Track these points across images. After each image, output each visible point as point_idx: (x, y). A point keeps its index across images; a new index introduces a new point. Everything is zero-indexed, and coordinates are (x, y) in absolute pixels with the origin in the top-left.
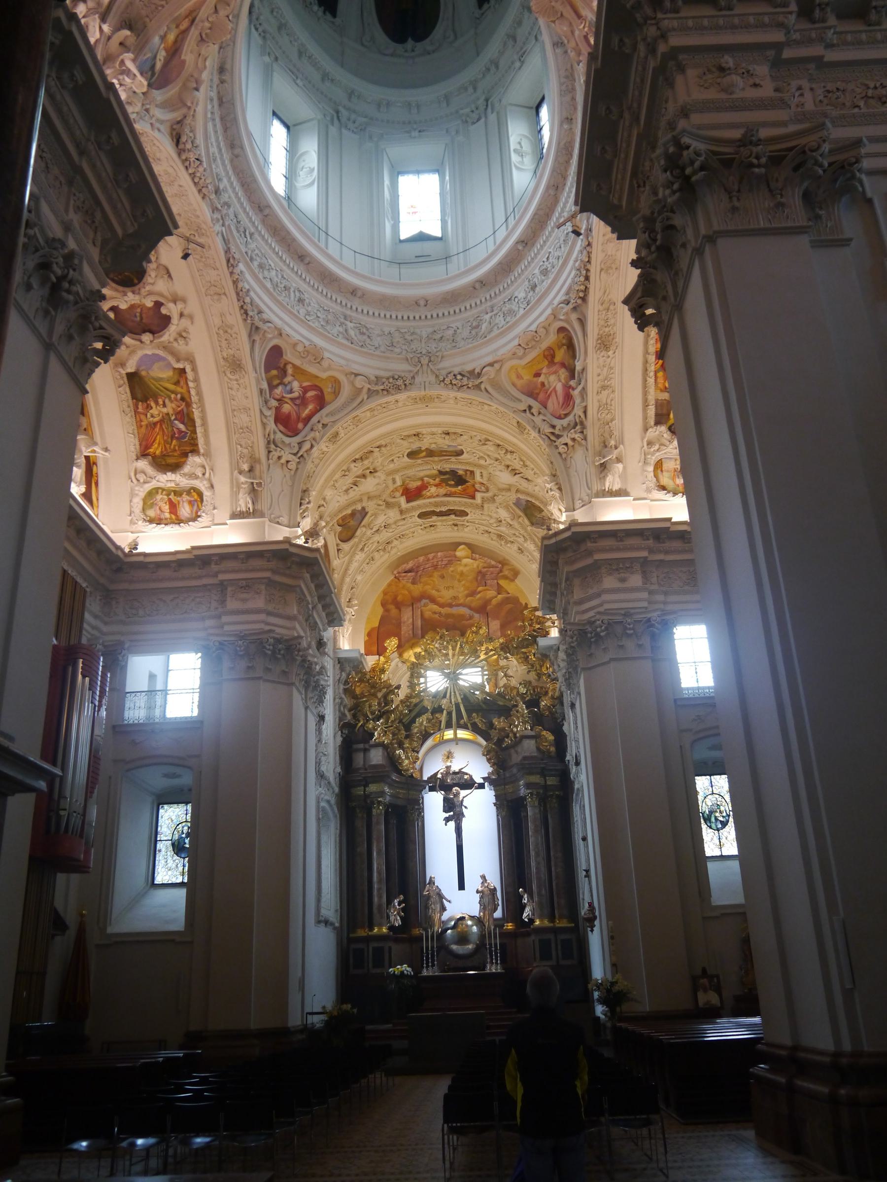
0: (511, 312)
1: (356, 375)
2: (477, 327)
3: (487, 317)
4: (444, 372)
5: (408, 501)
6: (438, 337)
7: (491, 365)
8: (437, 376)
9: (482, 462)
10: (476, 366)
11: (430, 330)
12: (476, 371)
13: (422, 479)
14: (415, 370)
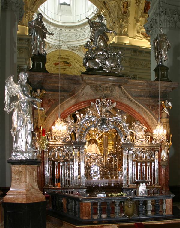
0: (84, 35)
1: (50, 44)
2: (77, 36)
3: (79, 34)
4: (69, 45)
5: (55, 65)
6: (68, 36)
7: (79, 46)
8: (67, 46)
9: (73, 62)
10: (76, 45)
11: (66, 33)
12: (76, 47)
13: (59, 62)
14: (62, 44)
